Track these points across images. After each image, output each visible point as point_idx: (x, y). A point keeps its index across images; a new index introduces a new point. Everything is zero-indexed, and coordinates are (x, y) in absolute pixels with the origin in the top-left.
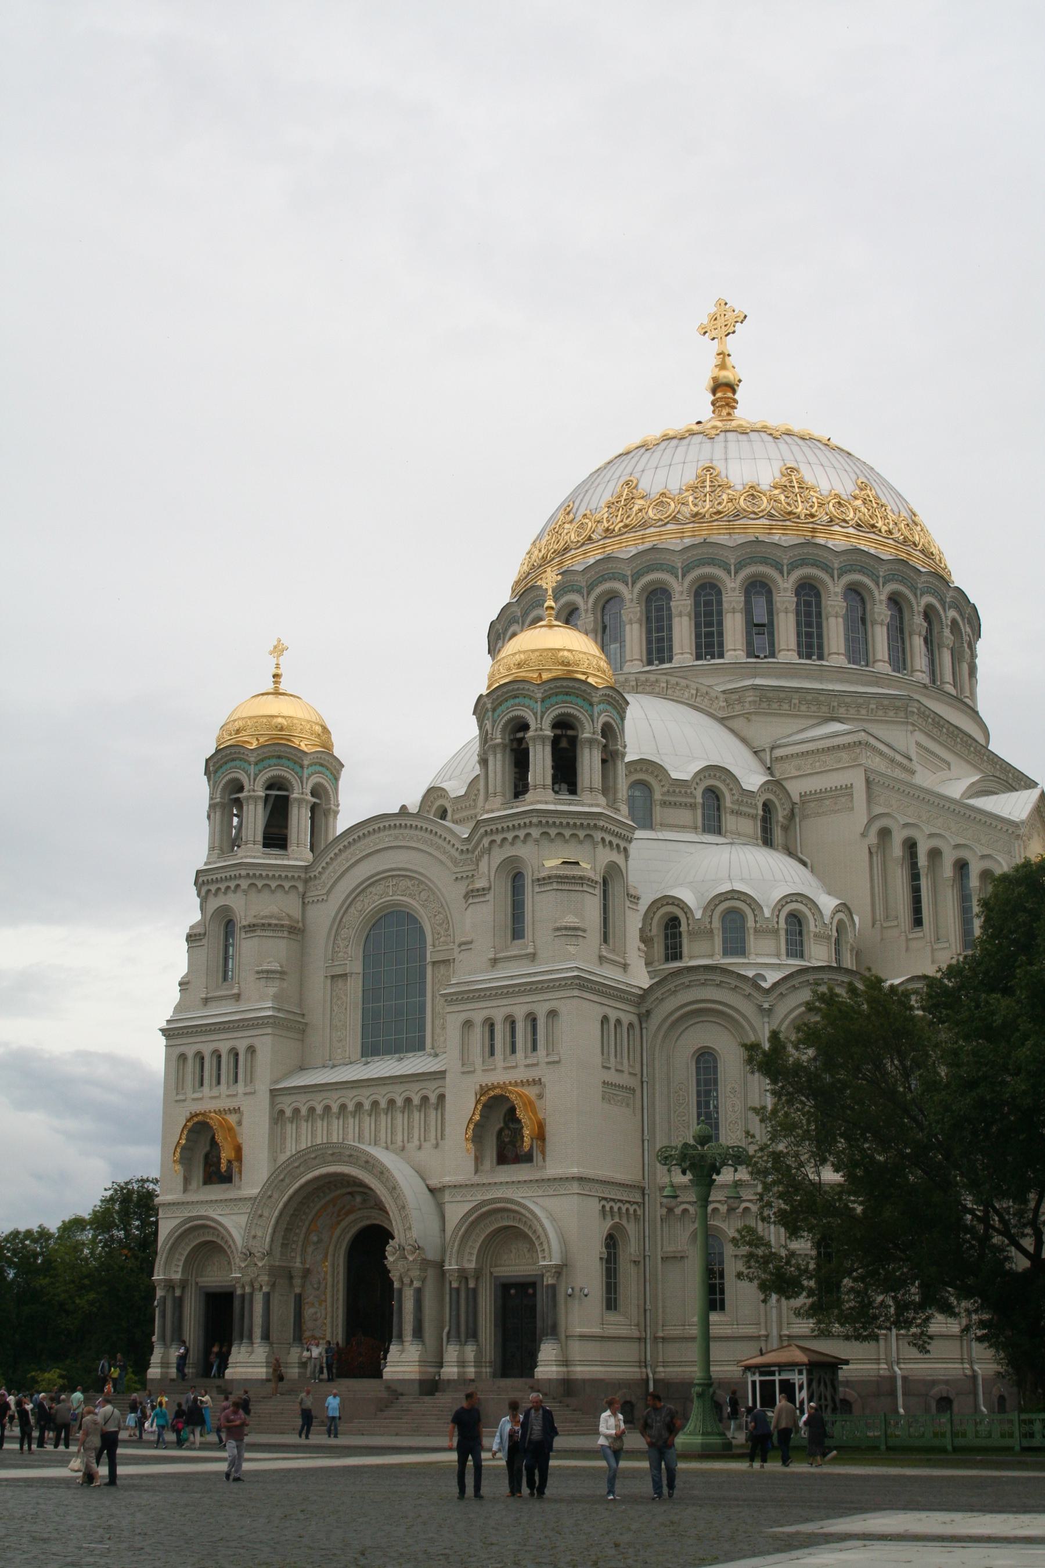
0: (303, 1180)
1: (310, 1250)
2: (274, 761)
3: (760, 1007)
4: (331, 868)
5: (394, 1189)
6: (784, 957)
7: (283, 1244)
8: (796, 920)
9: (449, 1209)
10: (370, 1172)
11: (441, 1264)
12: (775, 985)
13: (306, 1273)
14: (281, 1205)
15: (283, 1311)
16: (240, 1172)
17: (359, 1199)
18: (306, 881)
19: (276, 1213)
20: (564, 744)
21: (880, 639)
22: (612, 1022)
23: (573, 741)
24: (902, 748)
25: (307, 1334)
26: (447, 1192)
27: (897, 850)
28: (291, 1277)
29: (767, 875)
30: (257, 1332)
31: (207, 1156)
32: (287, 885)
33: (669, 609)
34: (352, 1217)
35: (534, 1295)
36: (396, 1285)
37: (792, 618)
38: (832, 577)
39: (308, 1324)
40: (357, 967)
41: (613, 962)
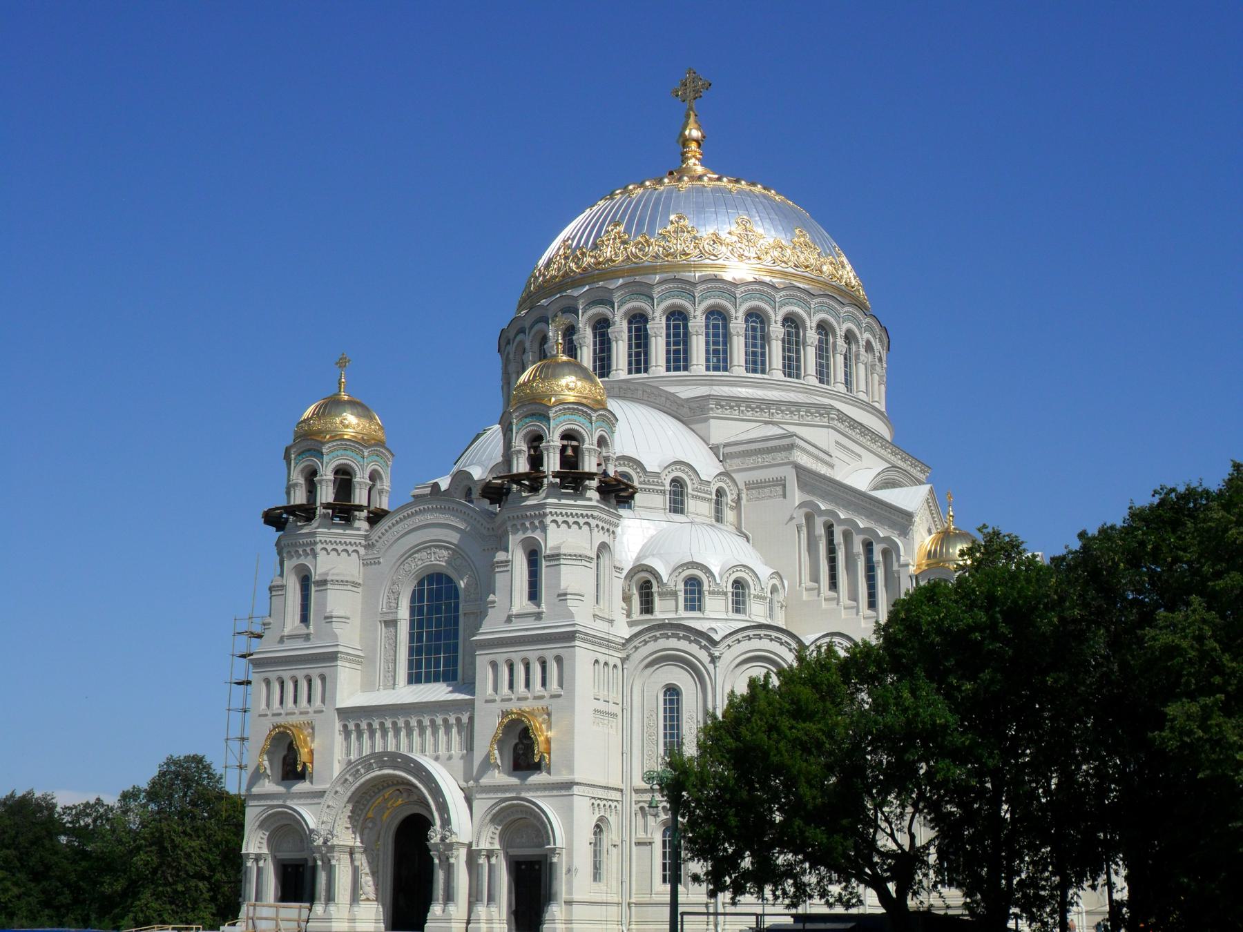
0: (363, 780)
2: (341, 452)
3: (711, 655)
4: (384, 538)
6: (730, 613)
8: (739, 584)
9: (475, 804)
12: (726, 637)
18: (365, 547)
20: (569, 452)
21: (810, 357)
22: (602, 664)
23: (576, 449)
24: (825, 448)
27: (820, 530)
29: (720, 551)
31: (284, 758)
32: (350, 549)
33: (646, 329)
35: (540, 869)
37: (742, 340)
38: (775, 308)
40: (404, 613)
41: (604, 619)
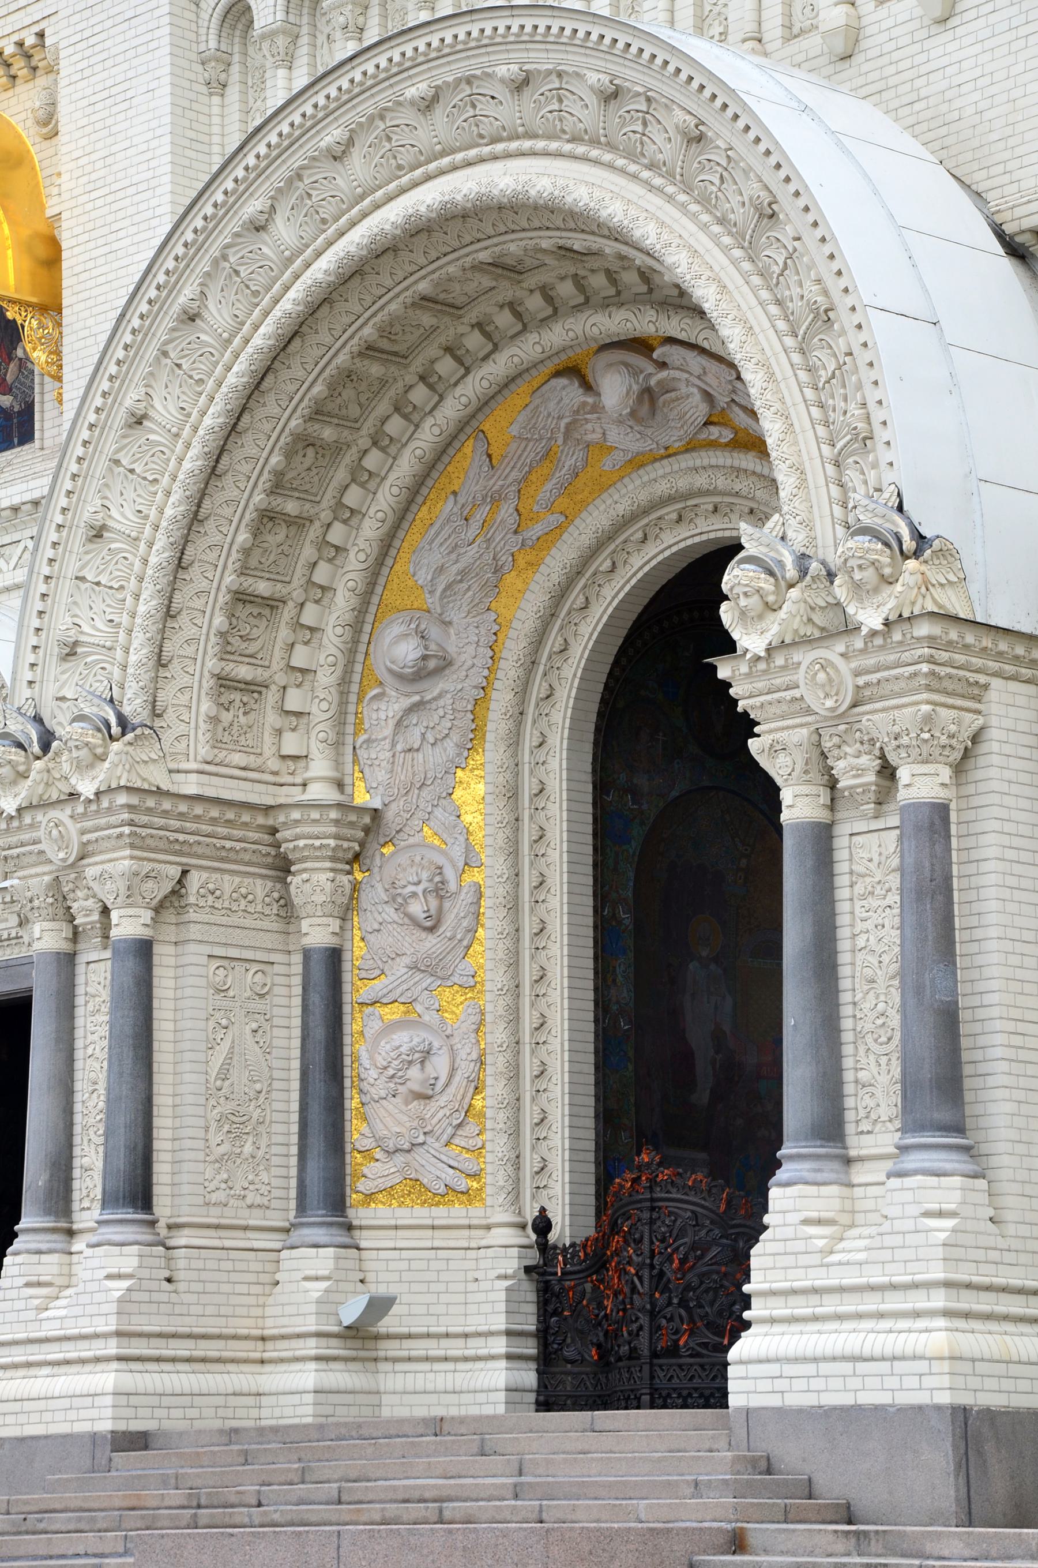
7: (224, 682)
13: (364, 835)
15: (223, 1052)
17: (615, 388)
28: (282, 867)
36: (798, 806)
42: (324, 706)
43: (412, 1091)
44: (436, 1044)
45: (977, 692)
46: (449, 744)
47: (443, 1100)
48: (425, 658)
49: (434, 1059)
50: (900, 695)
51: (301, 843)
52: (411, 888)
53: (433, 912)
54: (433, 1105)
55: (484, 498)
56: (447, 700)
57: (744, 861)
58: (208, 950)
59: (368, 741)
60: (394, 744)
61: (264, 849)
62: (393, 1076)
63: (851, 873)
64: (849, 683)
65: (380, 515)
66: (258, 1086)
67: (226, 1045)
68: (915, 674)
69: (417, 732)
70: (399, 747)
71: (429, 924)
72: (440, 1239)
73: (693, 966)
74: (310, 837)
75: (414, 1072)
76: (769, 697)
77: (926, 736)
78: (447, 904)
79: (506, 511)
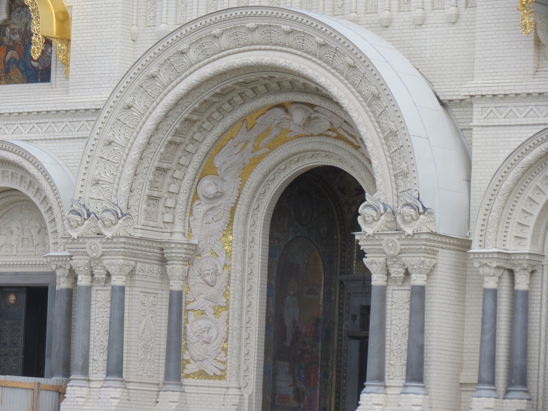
0: (194, 78)
1: (201, 208)
5: (377, 99)
7: (150, 197)
9: (478, 139)
10: (329, 64)
11: (464, 245)
13: (193, 253)
14: (150, 124)
15: (146, 324)
16: (66, 64)
17: (298, 116)
19: (141, 139)
25: (191, 368)
26: (477, 109)
28: (163, 261)
30: (98, 361)
34: (281, 152)
36: (377, 280)
39: (194, 349)
42: (182, 207)
43: (204, 341)
44: (212, 325)
45: (435, 253)
46: (221, 221)
47: (214, 344)
48: (217, 192)
49: (211, 330)
50: (414, 253)
51: (173, 255)
52: (207, 272)
53: (214, 280)
54: (210, 346)
55: (243, 141)
56: (222, 207)
57: (306, 261)
58: (140, 289)
59: (194, 219)
60: (203, 221)
61: (158, 255)
62: (198, 336)
63: (392, 301)
64: (399, 247)
65: (208, 144)
66: (152, 336)
67: (144, 322)
68: (420, 248)
69: (211, 217)
70: (204, 222)
71: (212, 284)
72: (212, 390)
73: (288, 297)
74: (176, 253)
75: (205, 335)
76: (372, 247)
77: (422, 266)
78: (218, 277)
79: (250, 146)
